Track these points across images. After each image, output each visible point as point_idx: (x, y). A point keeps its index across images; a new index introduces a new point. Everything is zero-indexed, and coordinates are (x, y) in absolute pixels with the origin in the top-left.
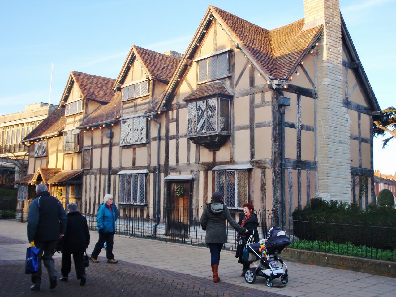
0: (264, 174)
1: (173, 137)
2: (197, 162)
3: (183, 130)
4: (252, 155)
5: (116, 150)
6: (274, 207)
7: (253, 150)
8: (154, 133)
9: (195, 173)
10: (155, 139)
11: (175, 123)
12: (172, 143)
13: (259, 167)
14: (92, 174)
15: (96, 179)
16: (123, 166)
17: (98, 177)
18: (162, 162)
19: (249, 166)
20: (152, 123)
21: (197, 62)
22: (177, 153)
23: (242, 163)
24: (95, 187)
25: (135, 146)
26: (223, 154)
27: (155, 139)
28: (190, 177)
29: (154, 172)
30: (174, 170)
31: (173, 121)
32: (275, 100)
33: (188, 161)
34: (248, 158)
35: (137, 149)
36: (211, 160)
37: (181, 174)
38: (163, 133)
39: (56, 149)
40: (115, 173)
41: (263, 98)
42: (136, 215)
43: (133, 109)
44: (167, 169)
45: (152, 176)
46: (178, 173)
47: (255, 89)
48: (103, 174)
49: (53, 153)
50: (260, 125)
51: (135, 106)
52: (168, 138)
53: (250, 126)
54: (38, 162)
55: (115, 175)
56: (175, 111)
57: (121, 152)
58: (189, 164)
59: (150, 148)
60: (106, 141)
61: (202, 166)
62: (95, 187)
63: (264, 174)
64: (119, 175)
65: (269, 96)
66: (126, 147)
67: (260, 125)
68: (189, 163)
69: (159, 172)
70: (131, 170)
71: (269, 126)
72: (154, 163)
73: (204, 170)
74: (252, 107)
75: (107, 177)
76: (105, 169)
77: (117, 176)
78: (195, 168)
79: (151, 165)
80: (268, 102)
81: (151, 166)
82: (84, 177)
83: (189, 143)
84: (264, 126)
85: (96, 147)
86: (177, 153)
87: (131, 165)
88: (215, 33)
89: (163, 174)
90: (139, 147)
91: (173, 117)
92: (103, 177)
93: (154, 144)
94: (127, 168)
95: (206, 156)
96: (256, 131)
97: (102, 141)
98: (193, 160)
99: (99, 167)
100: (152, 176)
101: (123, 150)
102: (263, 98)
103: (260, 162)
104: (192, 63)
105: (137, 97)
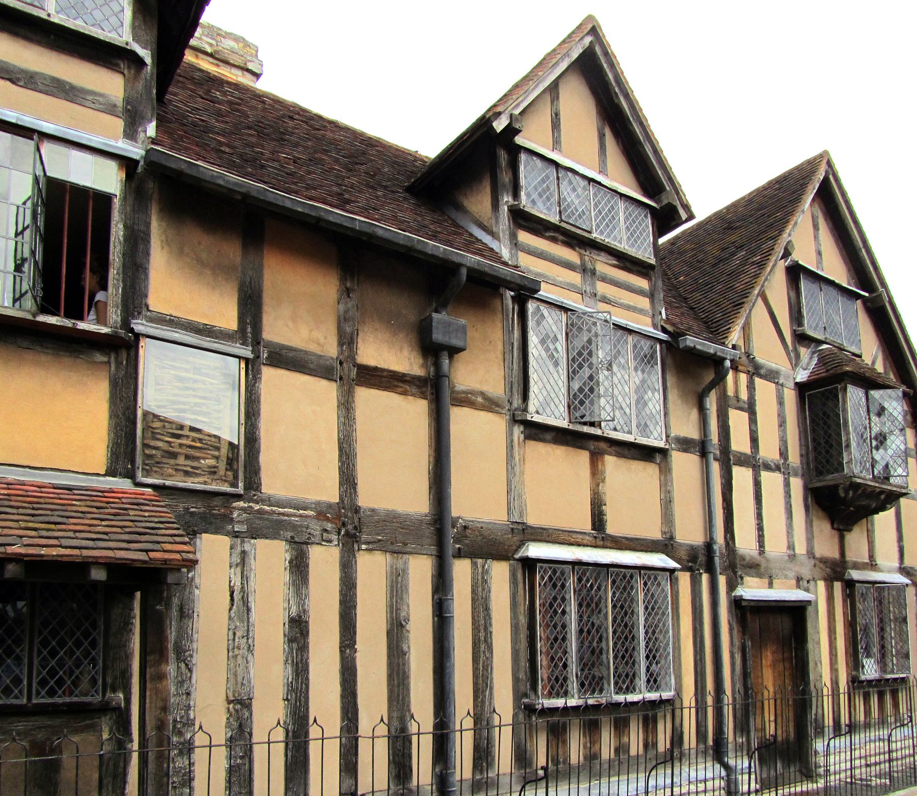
1: (743, 460)
2: (810, 553)
10: (685, 445)
11: (745, 416)
12: (742, 476)
14: (265, 527)
15: (299, 567)
16: (532, 520)
17: (324, 560)
22: (759, 516)
23: (890, 571)
25: (603, 445)
26: (856, 541)
27: (685, 445)
30: (754, 568)
33: (791, 547)
35: (610, 462)
36: (836, 555)
37: (774, 585)
40: (486, 546)
42: (621, 749)
46: (766, 581)
55: (480, 561)
56: (743, 378)
64: (529, 564)
66: (548, 436)
68: (792, 553)
70: (587, 546)
72: (690, 533)
73: (825, 580)
77: (500, 573)
78: (806, 571)
81: (681, 545)
87: (585, 524)
90: (620, 455)
94: (563, 537)
99: (331, 493)
101: (531, 444)
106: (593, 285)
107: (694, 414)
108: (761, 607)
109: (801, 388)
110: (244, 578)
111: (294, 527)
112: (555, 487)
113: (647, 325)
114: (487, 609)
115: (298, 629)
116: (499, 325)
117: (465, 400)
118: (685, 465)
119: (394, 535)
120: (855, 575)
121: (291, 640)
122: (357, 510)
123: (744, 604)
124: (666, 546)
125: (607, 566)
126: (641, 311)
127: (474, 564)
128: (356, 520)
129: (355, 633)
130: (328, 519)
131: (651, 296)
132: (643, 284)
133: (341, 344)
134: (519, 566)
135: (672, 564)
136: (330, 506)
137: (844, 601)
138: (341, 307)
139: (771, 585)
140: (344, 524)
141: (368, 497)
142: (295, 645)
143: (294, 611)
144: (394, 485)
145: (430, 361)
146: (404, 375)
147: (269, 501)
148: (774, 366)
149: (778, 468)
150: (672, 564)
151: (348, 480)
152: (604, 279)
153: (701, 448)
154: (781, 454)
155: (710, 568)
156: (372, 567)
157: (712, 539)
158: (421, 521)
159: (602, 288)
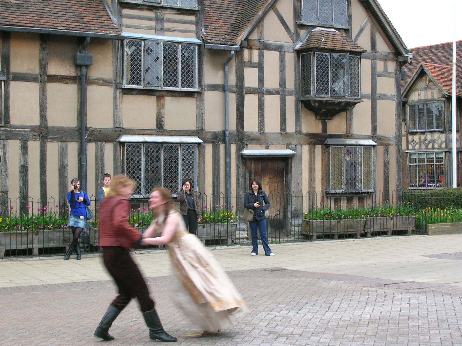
0: (387, 152)
1: (252, 91)
2: (298, 132)
3: (272, 81)
4: (374, 129)
6: (398, 187)
7: (375, 124)
9: (294, 147)
10: (213, 88)
11: (256, 70)
13: (381, 144)
15: (24, 149)
17: (34, 146)
18: (232, 126)
19: (372, 142)
20: (206, 59)
22: (261, 116)
26: (336, 126)
27: (213, 88)
28: (289, 152)
29: (213, 142)
30: (255, 140)
31: (251, 64)
32: (398, 73)
34: (369, 133)
35: (168, 100)
37: (270, 148)
38: (232, 80)
40: (102, 137)
41: (385, 67)
43: (153, 23)
44: (242, 139)
45: (209, 149)
47: (377, 54)
48: (53, 140)
50: (384, 97)
53: (372, 95)
55: (99, 143)
56: (256, 53)
59: (203, 100)
61: (307, 137)
63: (387, 152)
64: (122, 144)
65: (392, 66)
66: (134, 92)
67: (384, 97)
69: (230, 143)
71: (394, 100)
73: (309, 144)
74: (374, 74)
79: (207, 129)
80: (391, 73)
84: (388, 99)
86: (261, 116)
87: (153, 125)
89: (233, 148)
91: (251, 58)
94: (140, 132)
95: (311, 125)
96: (380, 103)
97: (43, 67)
98: (291, 128)
100: (209, 149)
102: (385, 67)
103: (383, 138)
105: (169, 5)
106: (162, 25)
107: (221, 73)
108: (256, 158)
109: (298, 52)
110: (5, 153)
111: (22, 135)
112: (139, 113)
113: (193, 37)
114: (102, 161)
115: (24, 169)
116: (111, 50)
117: (95, 82)
119: (62, 135)
120: (329, 141)
121: (21, 172)
122: (47, 127)
123: (244, 157)
124: (199, 133)
125: (162, 143)
126: (190, 32)
127: (97, 145)
128: (46, 131)
129: (46, 170)
130: (35, 131)
131: (197, 23)
132: (193, 18)
133: (41, 68)
134: (118, 144)
135: (200, 141)
136: (36, 127)
137: (323, 154)
138: (41, 55)
139: (267, 148)
140: (41, 133)
141: (52, 122)
142: (23, 174)
143: (23, 163)
144: (63, 116)
145: (78, 69)
146: (67, 76)
147: (13, 127)
148: (278, 43)
149: (277, 92)
150: (200, 141)
151: (43, 116)
152: (169, 21)
153: (223, 88)
154: (280, 85)
155: (224, 141)
156: (53, 148)
157: (226, 129)
158: (73, 130)
159: (167, 25)
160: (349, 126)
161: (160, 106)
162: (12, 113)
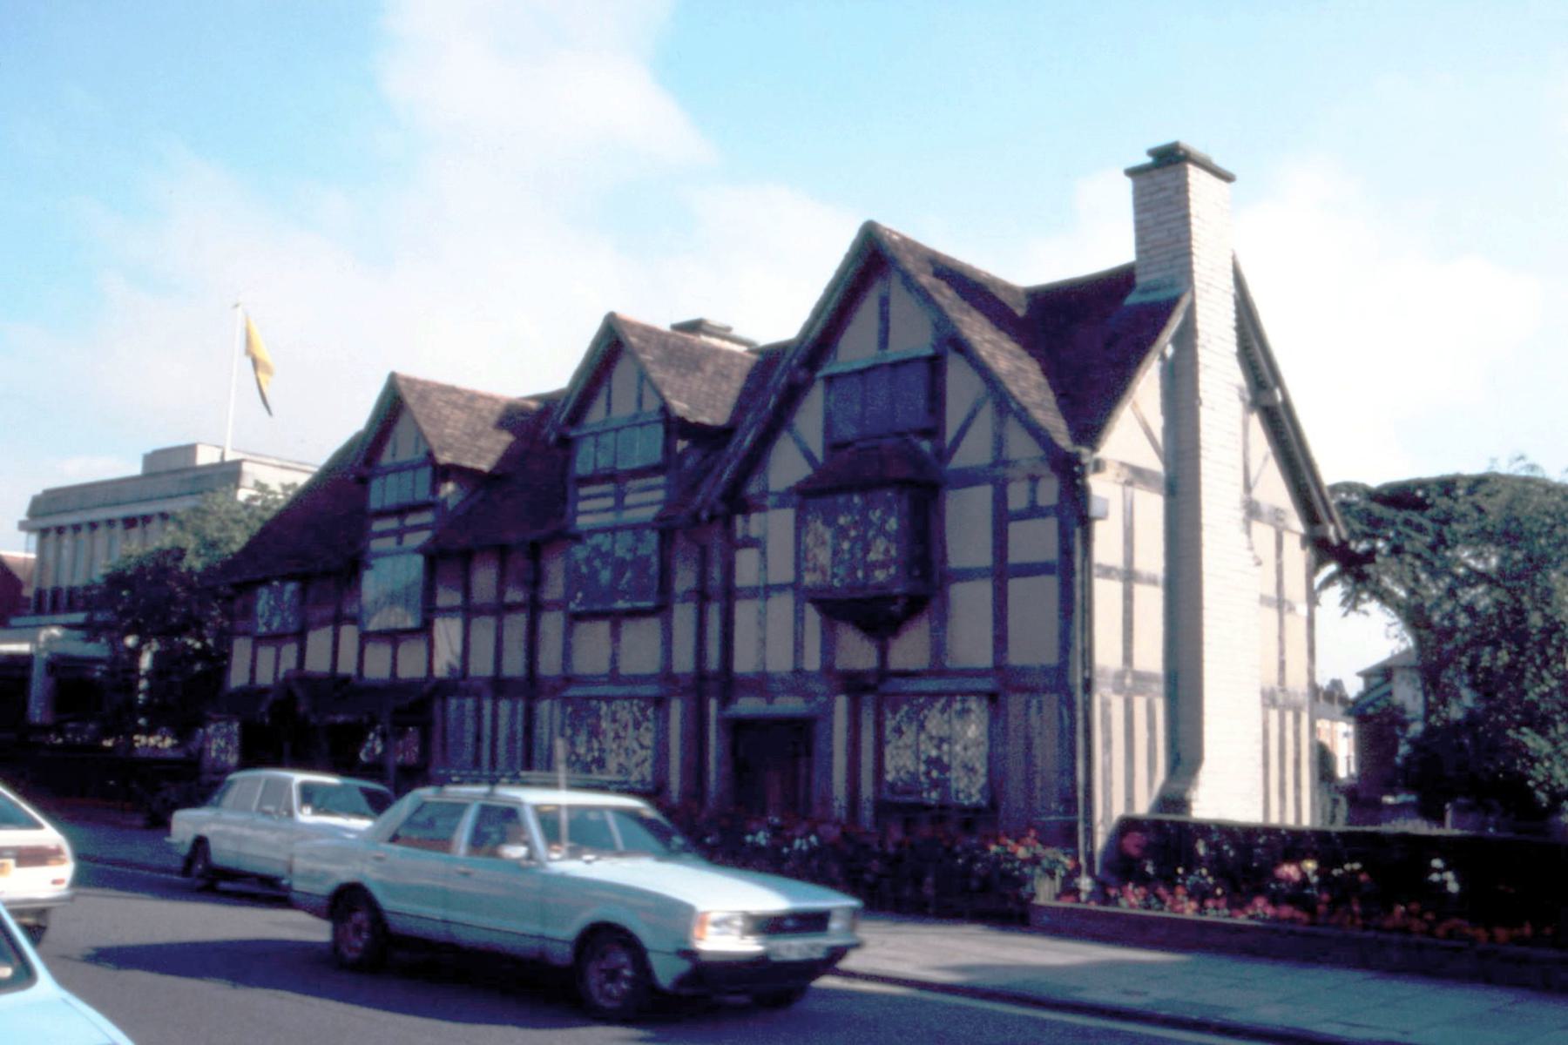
2: (828, 669)
5: (552, 624)
8: (685, 579)
12: (744, 612)
21: (830, 380)
24: (478, 738)
31: (750, 543)
39: (328, 612)
43: (610, 502)
44: (728, 683)
49: (323, 623)
51: (620, 497)
52: (730, 594)
54: (266, 654)
57: (568, 632)
58: (798, 671)
60: (514, 595)
62: (478, 738)
74: (1002, 518)
75: (520, 706)
76: (512, 680)
82: (437, 704)
83: (799, 618)
85: (480, 611)
88: (884, 302)
89: (713, 705)
92: (504, 706)
93: (684, 615)
95: (857, 653)
96: (1016, 586)
97: (501, 592)
98: (813, 662)
104: (810, 382)
118: (684, 615)
132: (661, 480)
160: (938, 648)
161: (615, 636)
162: (472, 659)
